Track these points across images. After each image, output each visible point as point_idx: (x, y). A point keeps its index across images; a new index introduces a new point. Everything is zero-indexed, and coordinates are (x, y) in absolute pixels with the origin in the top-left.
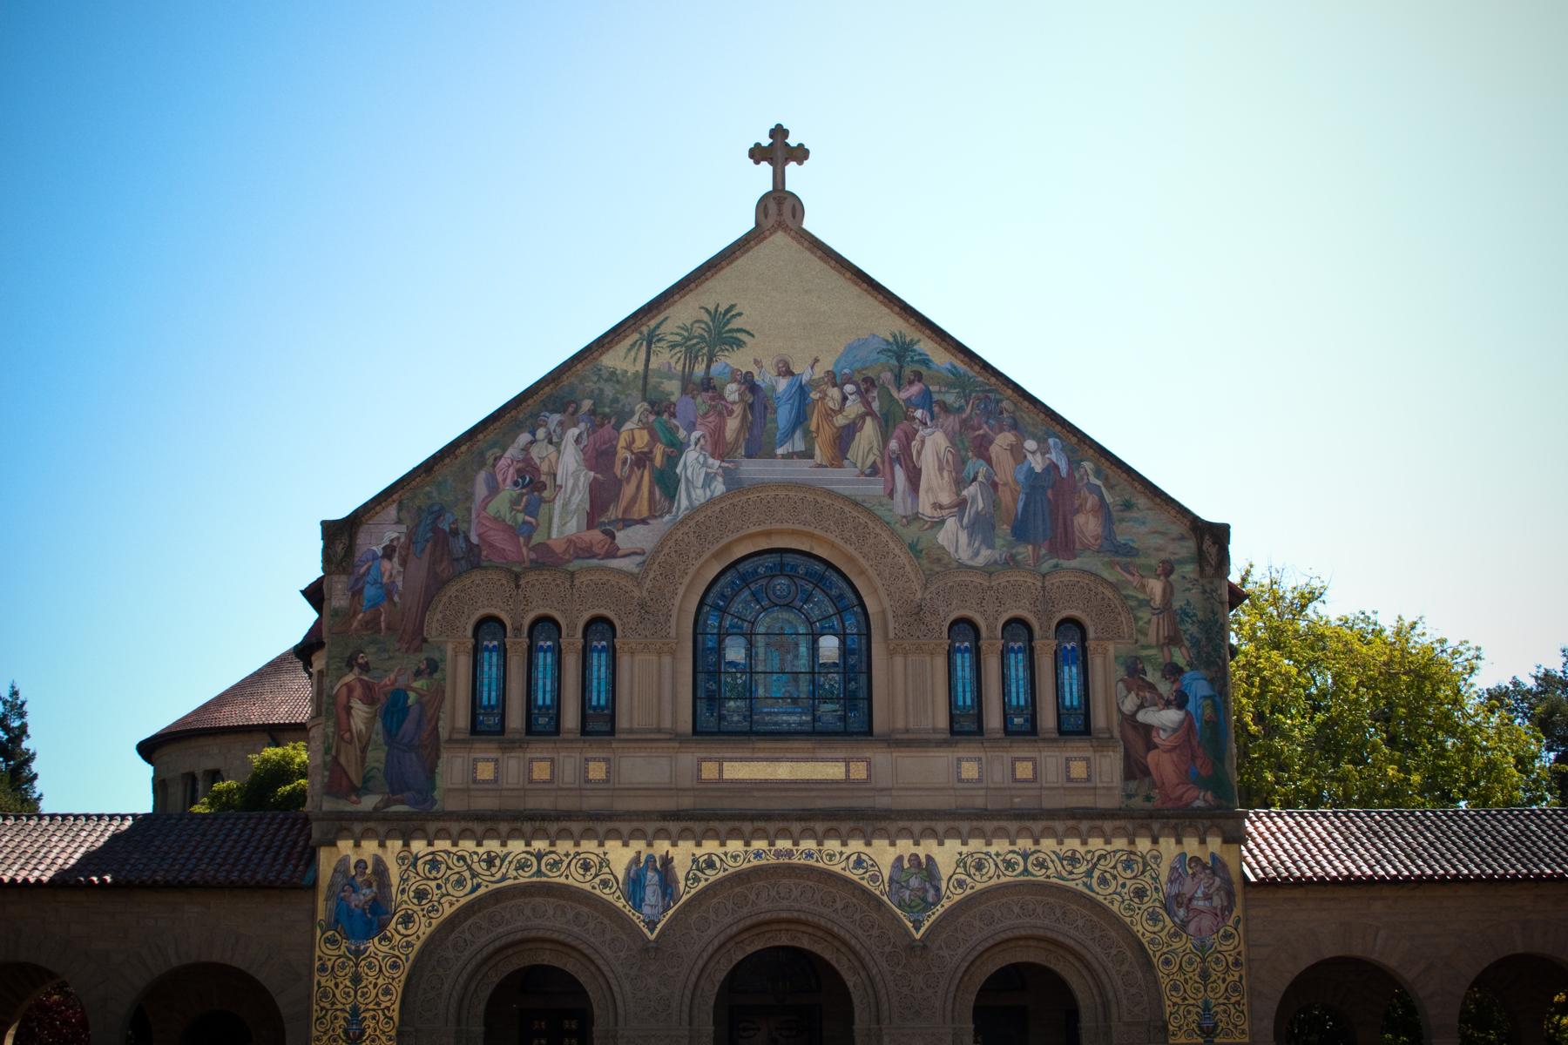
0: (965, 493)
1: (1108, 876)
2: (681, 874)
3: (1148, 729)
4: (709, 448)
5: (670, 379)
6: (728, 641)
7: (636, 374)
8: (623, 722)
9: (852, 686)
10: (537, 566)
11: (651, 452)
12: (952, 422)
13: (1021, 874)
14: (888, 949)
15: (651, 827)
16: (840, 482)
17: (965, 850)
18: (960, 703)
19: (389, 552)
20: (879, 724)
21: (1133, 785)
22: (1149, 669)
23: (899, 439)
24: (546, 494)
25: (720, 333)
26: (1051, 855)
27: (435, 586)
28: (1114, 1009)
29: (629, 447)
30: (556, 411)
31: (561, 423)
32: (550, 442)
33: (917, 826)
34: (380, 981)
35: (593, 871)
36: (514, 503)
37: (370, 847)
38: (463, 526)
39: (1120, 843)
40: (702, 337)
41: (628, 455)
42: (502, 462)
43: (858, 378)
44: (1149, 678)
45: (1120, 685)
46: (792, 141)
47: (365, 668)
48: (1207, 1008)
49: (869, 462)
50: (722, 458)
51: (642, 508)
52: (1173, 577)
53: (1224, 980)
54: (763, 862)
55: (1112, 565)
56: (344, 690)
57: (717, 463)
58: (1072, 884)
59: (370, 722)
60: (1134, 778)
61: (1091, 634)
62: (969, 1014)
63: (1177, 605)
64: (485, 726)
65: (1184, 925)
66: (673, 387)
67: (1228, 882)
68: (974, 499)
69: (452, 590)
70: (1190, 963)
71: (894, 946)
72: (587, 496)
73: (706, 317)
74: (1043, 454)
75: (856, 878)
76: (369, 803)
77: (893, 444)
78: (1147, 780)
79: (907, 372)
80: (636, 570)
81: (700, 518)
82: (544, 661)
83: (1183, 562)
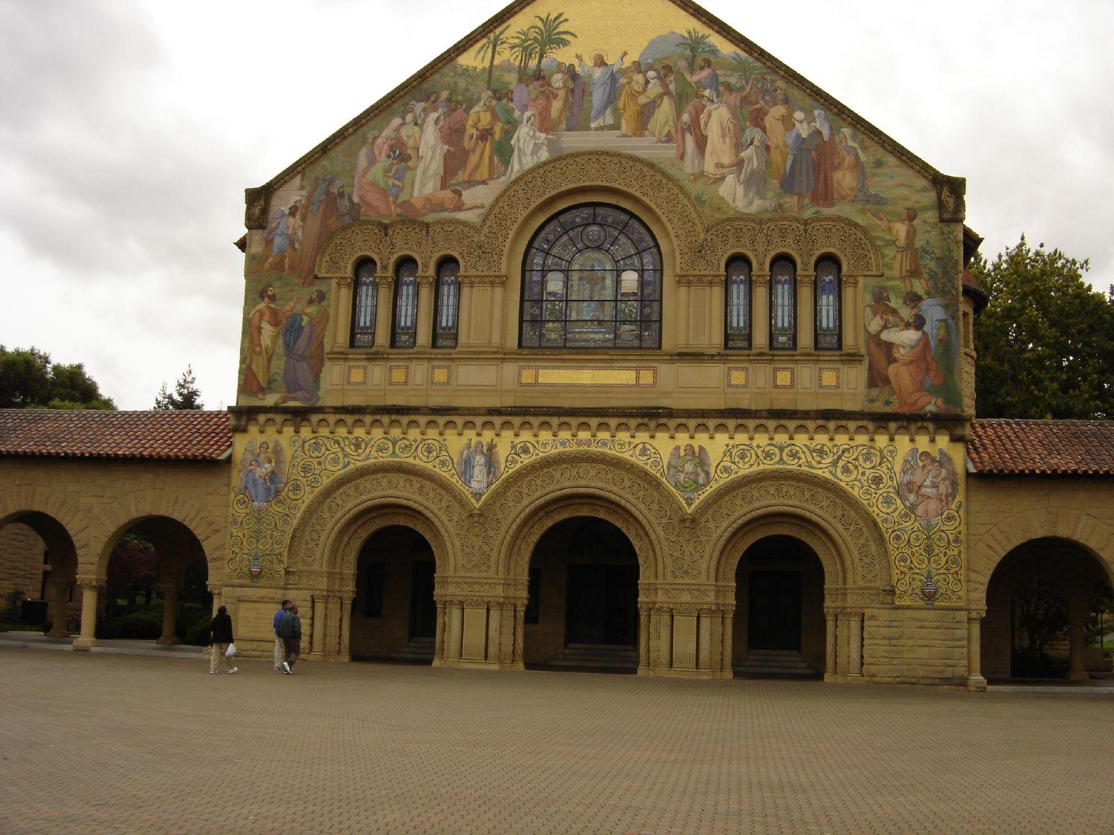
0: (743, 154)
1: (850, 465)
2: (502, 460)
3: (889, 346)
4: (537, 124)
5: (510, 71)
6: (550, 276)
7: (484, 70)
8: (462, 339)
9: (647, 311)
11: (492, 129)
12: (734, 98)
13: (778, 463)
14: (664, 520)
15: (479, 421)
16: (641, 148)
17: (731, 442)
18: (735, 324)
20: (667, 344)
21: (875, 392)
22: (892, 297)
23: (690, 114)
24: (410, 163)
25: (550, 35)
28: (850, 575)
29: (475, 126)
30: (422, 101)
31: (425, 110)
32: (416, 124)
33: (692, 423)
34: (275, 533)
35: (434, 454)
36: (387, 171)
37: (271, 434)
38: (347, 190)
39: (862, 439)
40: (535, 39)
41: (474, 132)
42: (379, 141)
43: (659, 66)
44: (892, 304)
45: (868, 310)
47: (273, 298)
48: (929, 577)
49: (665, 132)
50: (547, 131)
51: (483, 173)
52: (915, 222)
53: (945, 554)
54: (568, 449)
55: (863, 212)
56: (257, 315)
57: (543, 135)
58: (819, 472)
59: (274, 339)
60: (877, 387)
61: (845, 268)
62: (733, 575)
63: (918, 244)
65: (913, 508)
66: (511, 78)
67: (954, 473)
68: (750, 159)
70: (917, 539)
71: (670, 518)
72: (442, 164)
73: (540, 24)
74: (809, 123)
75: (641, 463)
76: (271, 400)
77: (686, 117)
78: (887, 388)
79: (699, 61)
80: (477, 220)
81: (529, 178)
83: (925, 209)
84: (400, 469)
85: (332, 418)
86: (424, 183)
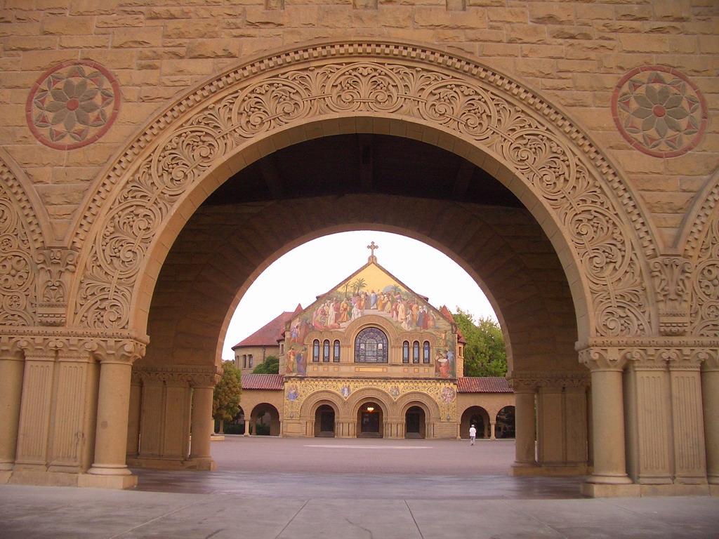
8: (341, 360)
19: (297, 327)
26: (423, 388)
27: (306, 334)
37: (294, 383)
39: (434, 384)
46: (375, 245)
64: (316, 360)
69: (309, 335)
76: (294, 375)
82: (326, 348)
84: (327, 391)
85: (310, 379)
86: (330, 321)
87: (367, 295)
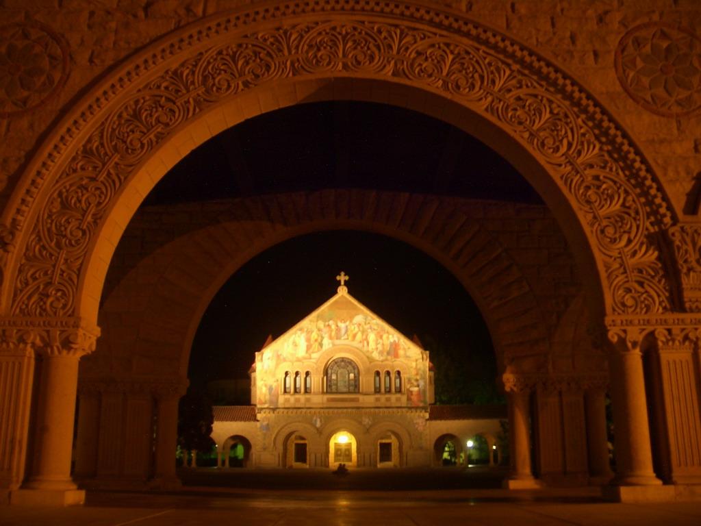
3: (411, 392)
8: (312, 391)
10: (297, 361)
12: (375, 332)
20: (361, 391)
27: (277, 365)
47: (265, 381)
51: (316, 350)
76: (266, 406)
87: (337, 326)
